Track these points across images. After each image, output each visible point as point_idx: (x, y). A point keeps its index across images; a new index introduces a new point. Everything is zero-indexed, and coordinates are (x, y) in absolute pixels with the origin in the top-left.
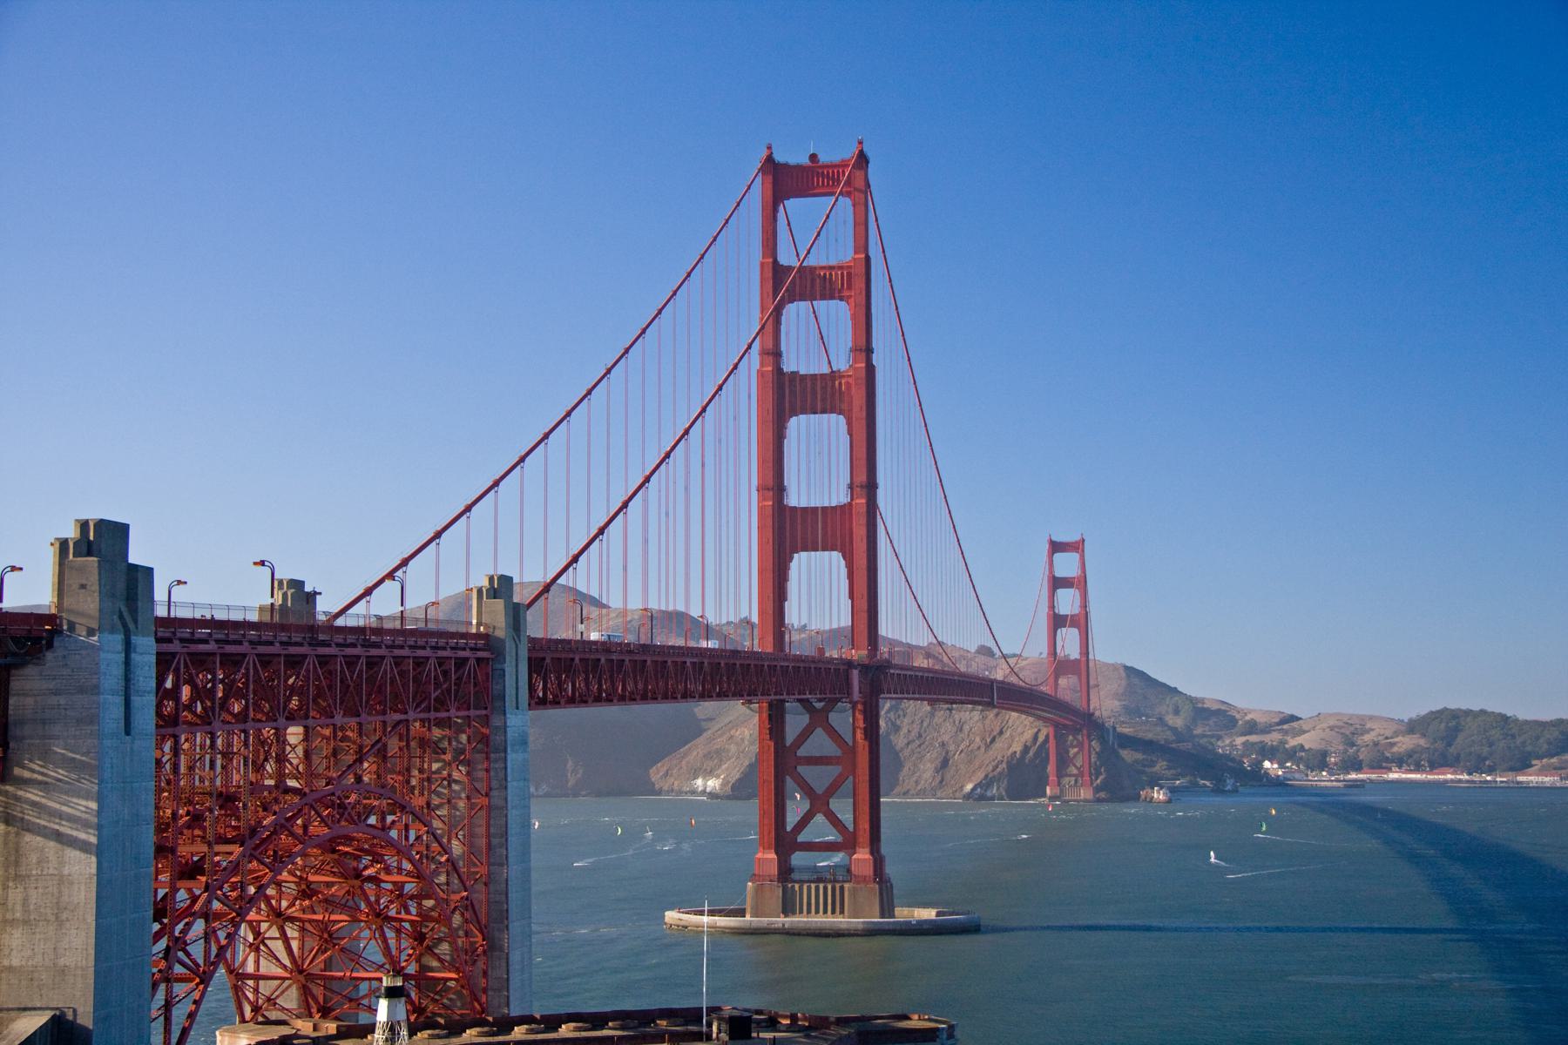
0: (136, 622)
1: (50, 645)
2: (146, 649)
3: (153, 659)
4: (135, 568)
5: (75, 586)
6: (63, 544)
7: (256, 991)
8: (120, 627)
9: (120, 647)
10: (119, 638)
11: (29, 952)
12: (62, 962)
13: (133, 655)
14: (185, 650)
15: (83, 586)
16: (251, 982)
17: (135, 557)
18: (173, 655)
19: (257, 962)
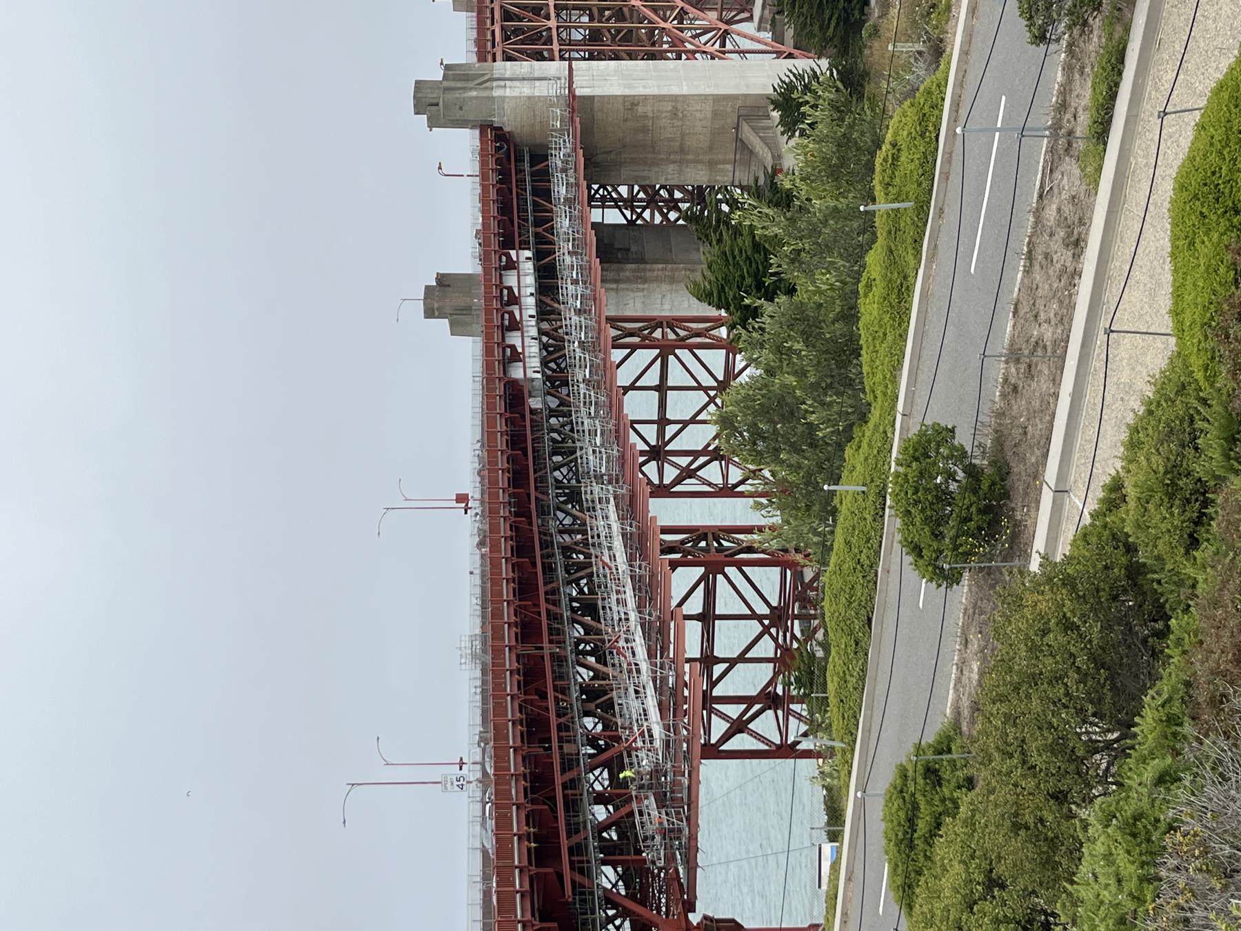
0: (483, 75)
1: (501, 129)
2: (503, 68)
3: (509, 63)
4: (445, 77)
5: (461, 112)
6: (432, 124)
7: (730, 10)
8: (488, 84)
9: (502, 83)
10: (495, 84)
11: (701, 136)
12: (709, 115)
13: (507, 76)
14: (500, 44)
15: (461, 108)
16: (724, 13)
17: (438, 75)
18: (504, 52)
19: (710, 9)
